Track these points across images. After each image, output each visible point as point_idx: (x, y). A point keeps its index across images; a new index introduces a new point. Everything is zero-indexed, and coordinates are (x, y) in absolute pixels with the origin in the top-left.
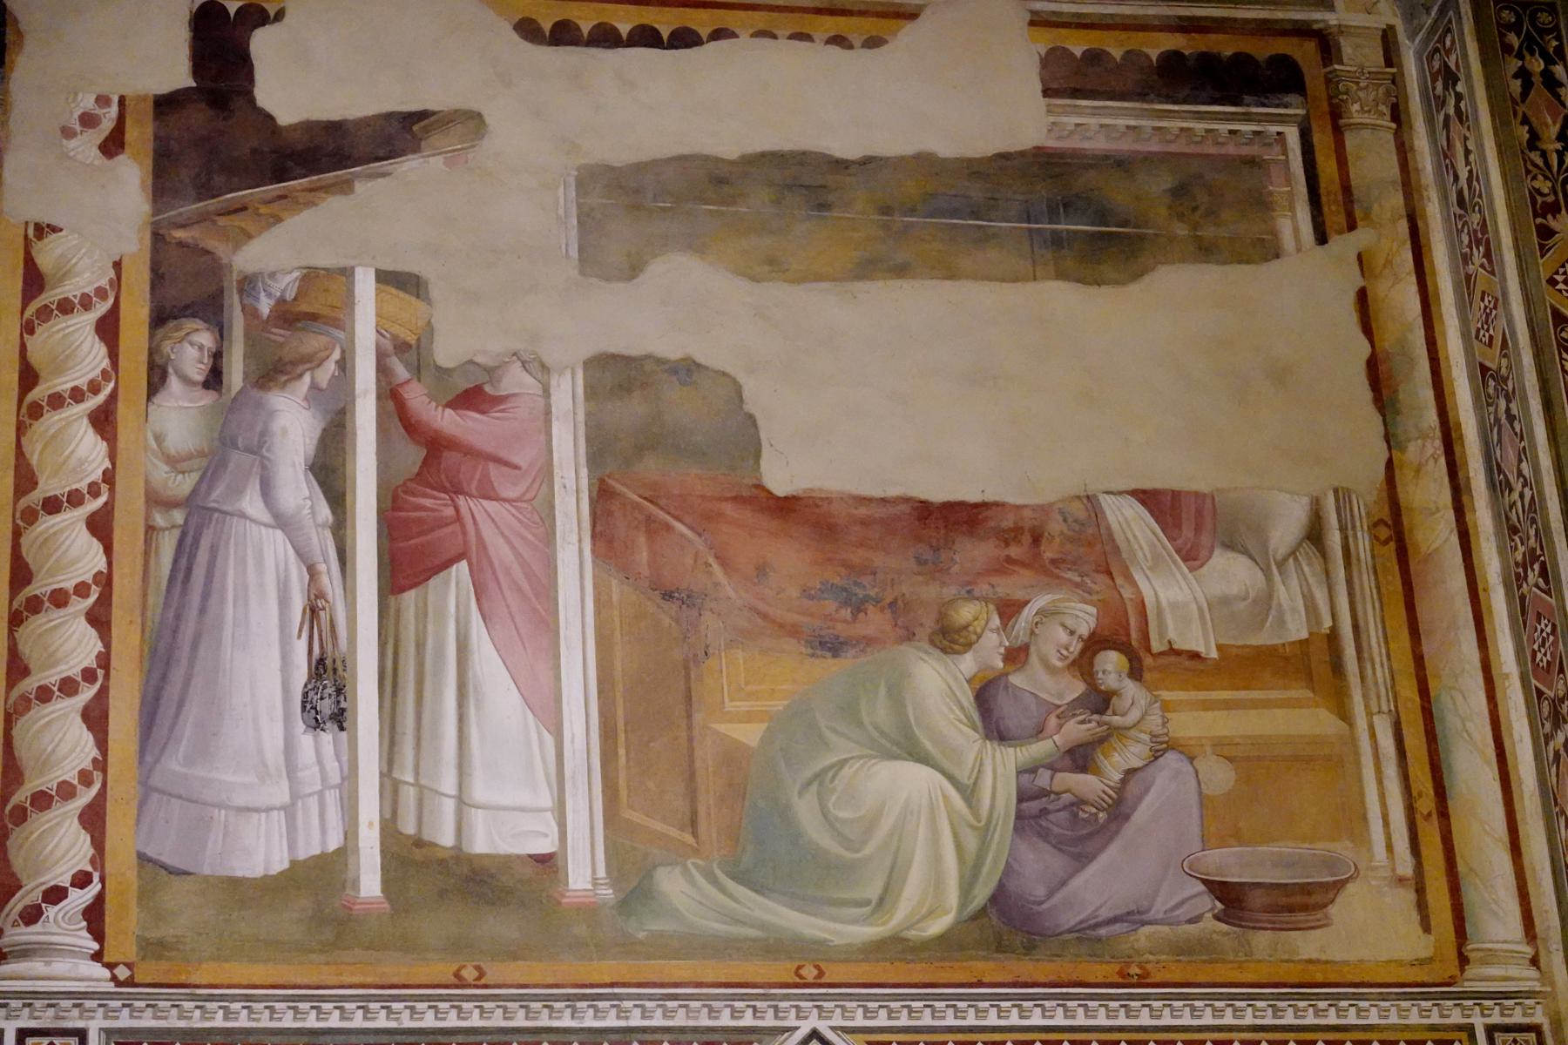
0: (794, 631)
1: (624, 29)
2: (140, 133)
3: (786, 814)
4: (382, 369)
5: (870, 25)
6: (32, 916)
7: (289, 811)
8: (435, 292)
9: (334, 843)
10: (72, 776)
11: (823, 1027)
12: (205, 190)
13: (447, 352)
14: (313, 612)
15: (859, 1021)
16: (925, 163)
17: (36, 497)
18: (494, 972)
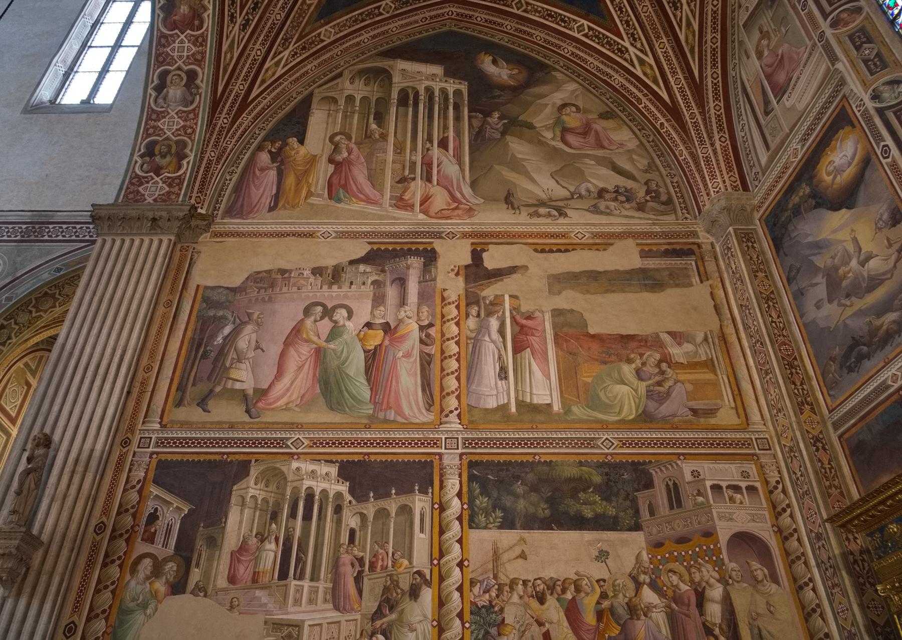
0: (597, 360)
1: (555, 249)
2: (462, 272)
3: (598, 395)
4: (511, 313)
5: (604, 247)
6: (447, 416)
7: (497, 395)
8: (521, 298)
9: (506, 401)
10: (454, 390)
11: (608, 437)
12: (475, 282)
13: (524, 309)
14: (499, 358)
15: (616, 436)
16: (617, 271)
17: (445, 338)
18: (539, 426)
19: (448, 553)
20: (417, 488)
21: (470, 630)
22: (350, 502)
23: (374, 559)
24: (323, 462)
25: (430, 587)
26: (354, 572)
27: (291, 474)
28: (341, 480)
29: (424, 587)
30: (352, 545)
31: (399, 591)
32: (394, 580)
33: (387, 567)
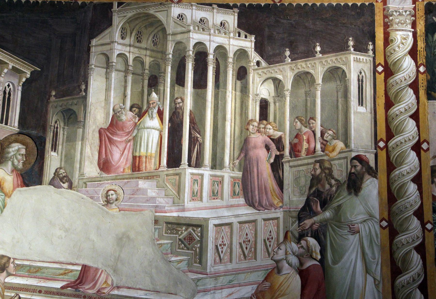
19: (400, 132)
20: (351, 43)
21: (433, 233)
22: (258, 63)
23: (296, 141)
24: (215, 6)
25: (376, 177)
26: (270, 157)
27: (172, 24)
28: (243, 33)
29: (367, 176)
30: (265, 122)
31: (333, 182)
32: (325, 168)
33: (314, 151)
